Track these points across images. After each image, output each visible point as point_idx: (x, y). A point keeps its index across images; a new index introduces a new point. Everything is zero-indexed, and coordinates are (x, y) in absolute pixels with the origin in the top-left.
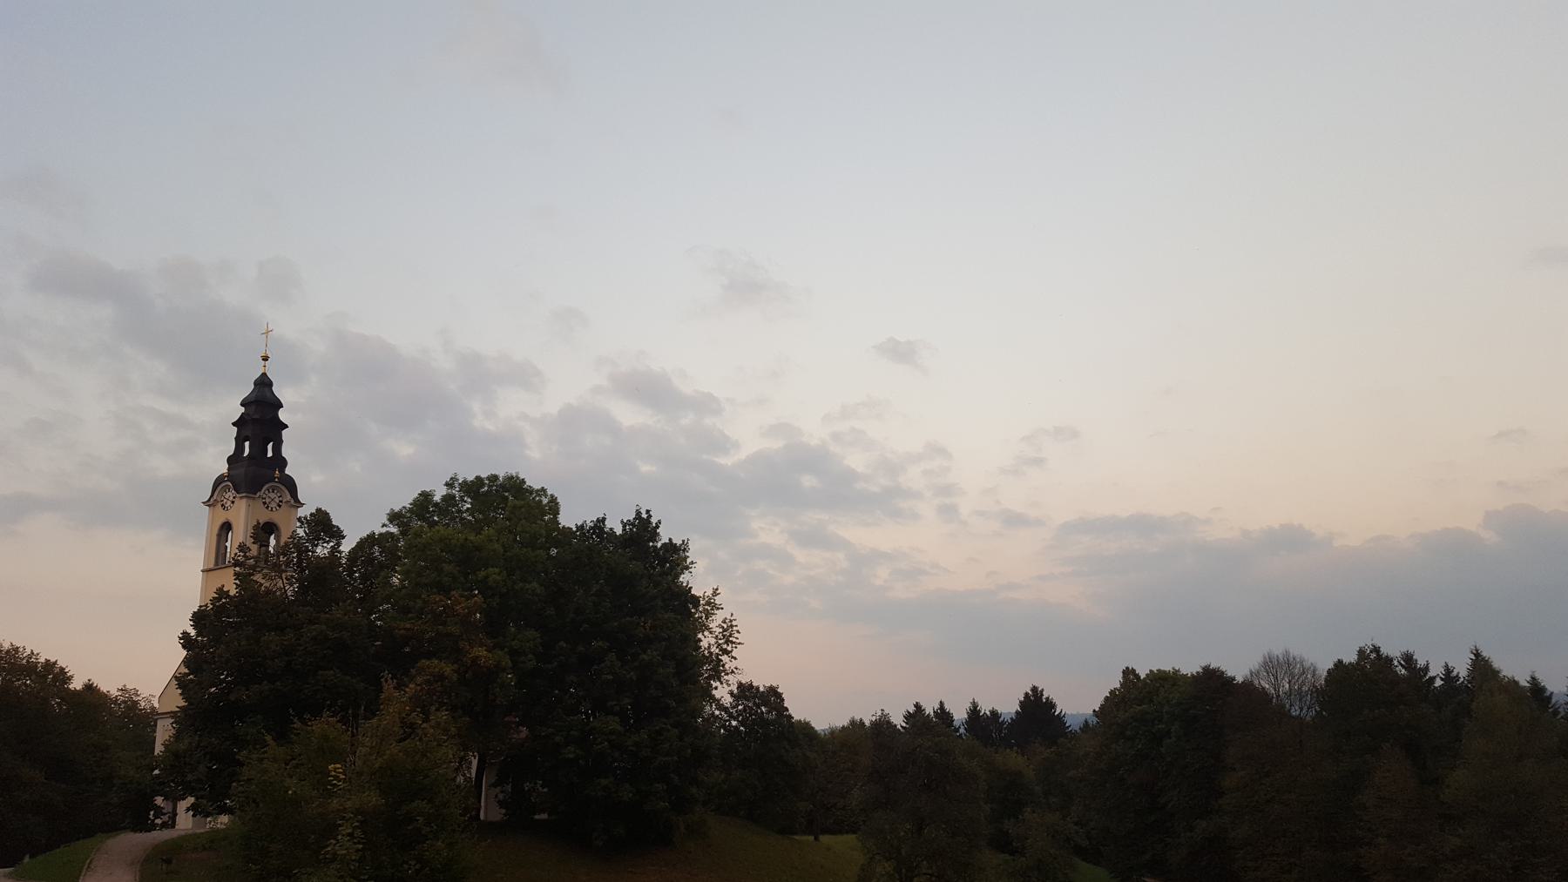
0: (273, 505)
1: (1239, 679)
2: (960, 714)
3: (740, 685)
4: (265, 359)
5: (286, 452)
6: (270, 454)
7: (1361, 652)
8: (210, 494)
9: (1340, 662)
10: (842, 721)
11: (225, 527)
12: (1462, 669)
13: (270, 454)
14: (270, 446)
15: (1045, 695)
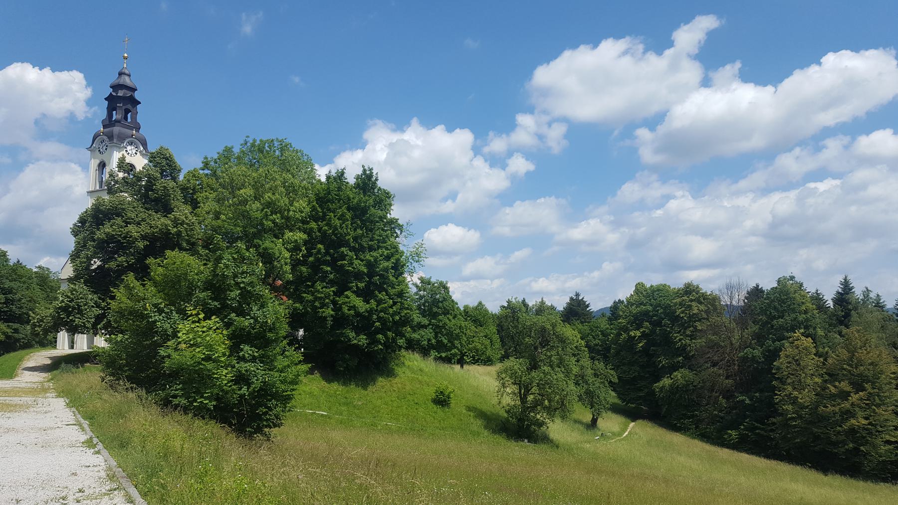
4: (127, 59)
11: (101, 165)
13: (129, 120)
14: (129, 115)
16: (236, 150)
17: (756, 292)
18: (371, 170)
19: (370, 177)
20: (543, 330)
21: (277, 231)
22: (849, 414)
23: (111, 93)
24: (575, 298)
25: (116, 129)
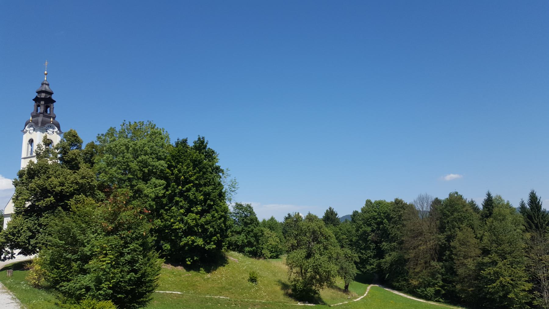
8: (24, 128)
10: (267, 218)
13: (48, 112)
14: (48, 109)
15: (334, 210)
16: (118, 129)
17: (437, 201)
18: (203, 138)
19: (203, 142)
20: (314, 232)
21: (146, 179)
22: (497, 275)
23: (37, 96)
25: (40, 119)
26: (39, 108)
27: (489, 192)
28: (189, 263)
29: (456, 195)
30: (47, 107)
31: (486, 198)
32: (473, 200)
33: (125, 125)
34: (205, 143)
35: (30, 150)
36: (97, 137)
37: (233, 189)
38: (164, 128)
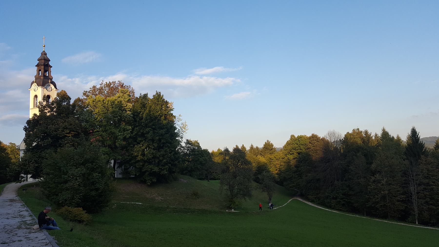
0: (50, 89)
1: (321, 138)
2: (248, 148)
3: (187, 140)
4: (44, 47)
5: (52, 75)
6: (47, 75)
7: (354, 130)
9: (348, 133)
12: (380, 134)
13: (47, 75)
14: (47, 72)
15: (271, 142)
18: (160, 93)
23: (38, 64)
24: (267, 142)
26: (40, 72)
27: (383, 128)
28: (149, 184)
29: (357, 131)
30: (45, 71)
31: (381, 133)
32: (377, 134)
33: (103, 84)
34: (161, 96)
35: (35, 103)
36: (83, 93)
37: (184, 130)
38: (130, 85)
